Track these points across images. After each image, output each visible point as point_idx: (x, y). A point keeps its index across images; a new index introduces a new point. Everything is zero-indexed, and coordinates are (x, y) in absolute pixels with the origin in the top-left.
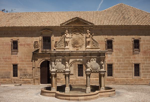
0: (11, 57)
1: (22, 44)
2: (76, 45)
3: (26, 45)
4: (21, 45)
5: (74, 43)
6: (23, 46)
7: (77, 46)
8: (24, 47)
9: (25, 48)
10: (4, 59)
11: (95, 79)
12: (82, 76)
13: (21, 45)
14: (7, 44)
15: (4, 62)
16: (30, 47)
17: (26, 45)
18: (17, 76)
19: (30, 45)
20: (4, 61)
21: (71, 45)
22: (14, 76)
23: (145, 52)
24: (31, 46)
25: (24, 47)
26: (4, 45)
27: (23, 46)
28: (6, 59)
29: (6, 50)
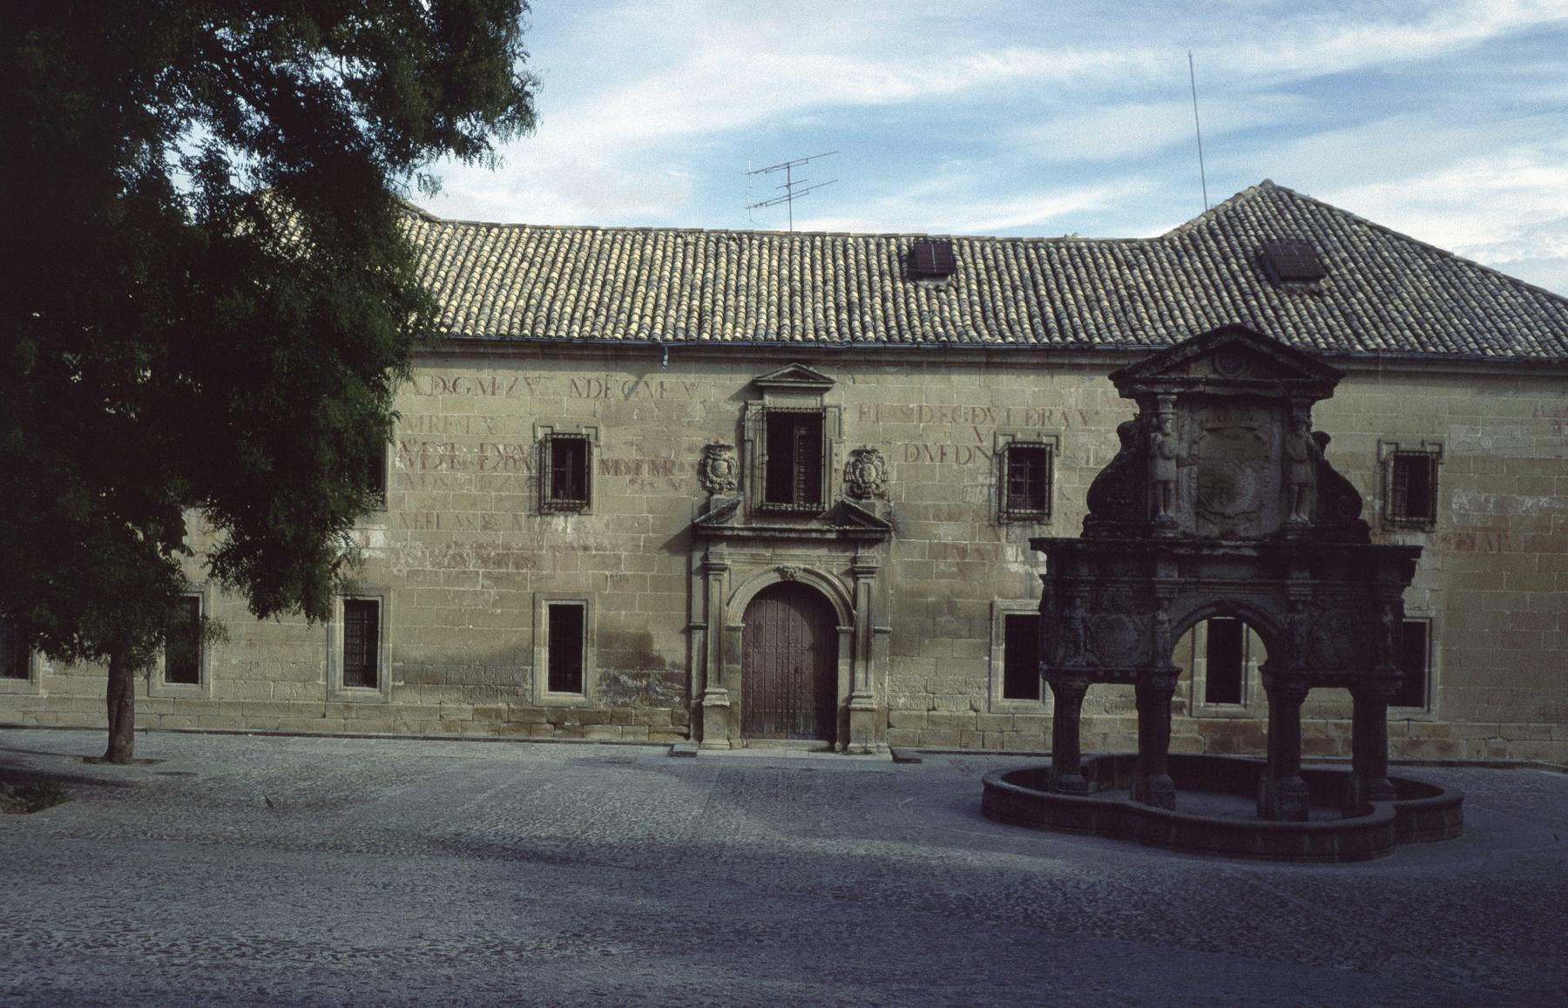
0: (541, 548)
1: (617, 462)
2: (1217, 507)
3: (645, 469)
4: (612, 467)
6: (628, 477)
7: (1229, 511)
8: (632, 481)
9: (636, 487)
10: (485, 561)
11: (1118, 717)
12: (1033, 694)
13: (612, 467)
14: (511, 462)
15: (487, 583)
16: (675, 487)
17: (645, 469)
18: (575, 685)
19: (675, 471)
20: (488, 576)
22: (555, 685)
23: (1464, 541)
24: (678, 476)
25: (632, 481)
26: (488, 465)
27: (628, 477)
28: (499, 564)
29: (500, 499)
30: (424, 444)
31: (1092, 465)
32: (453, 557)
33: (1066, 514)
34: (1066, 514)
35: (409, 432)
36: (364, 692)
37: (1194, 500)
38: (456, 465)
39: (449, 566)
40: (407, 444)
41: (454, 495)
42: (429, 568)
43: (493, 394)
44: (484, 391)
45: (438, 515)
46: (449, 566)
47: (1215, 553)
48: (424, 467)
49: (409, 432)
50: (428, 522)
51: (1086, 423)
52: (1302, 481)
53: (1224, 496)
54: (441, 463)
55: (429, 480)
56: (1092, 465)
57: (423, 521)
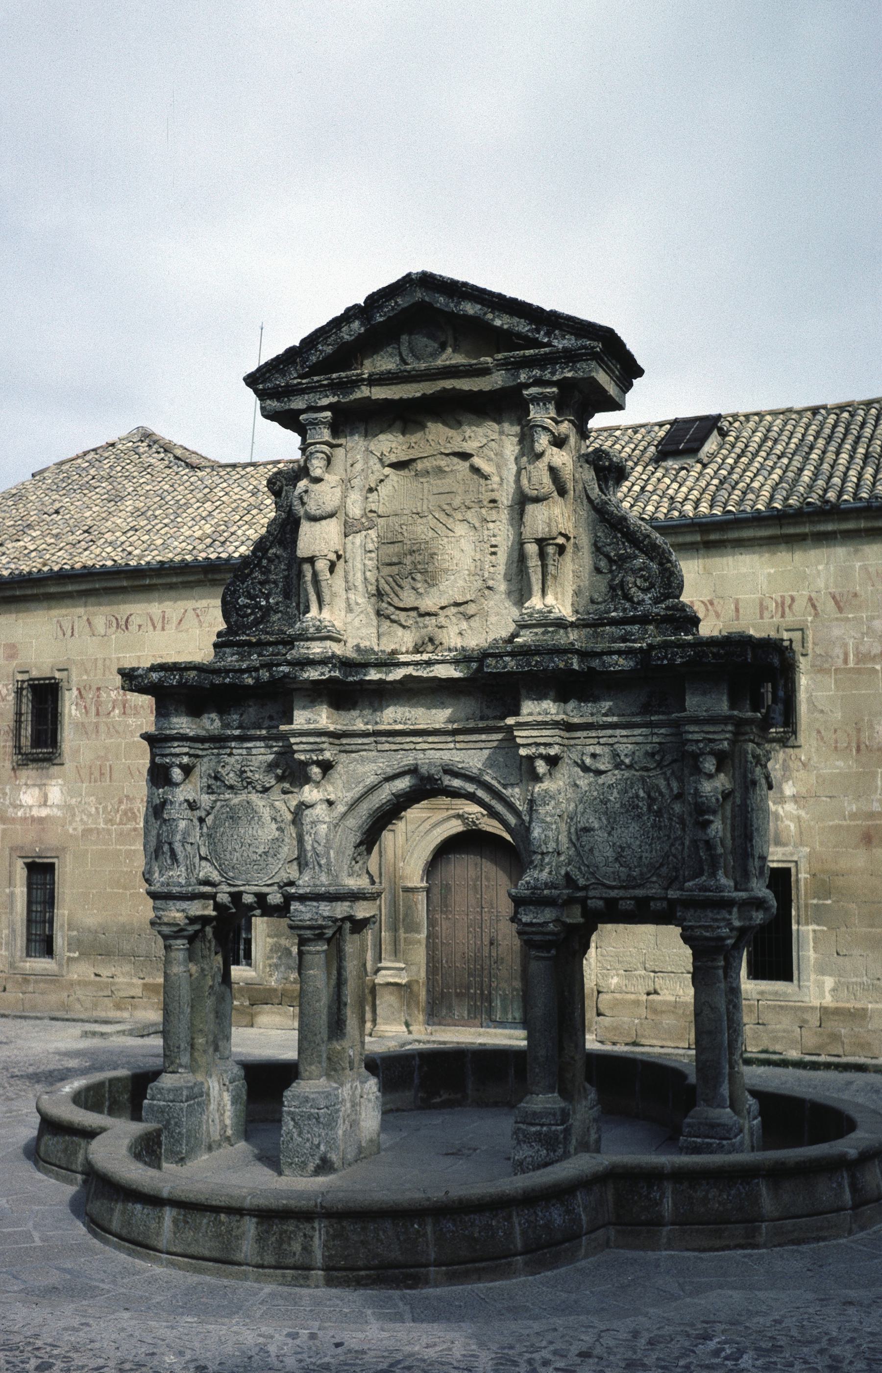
2: (408, 599)
5: (395, 569)
7: (428, 603)
21: (360, 598)
30: (99, 689)
31: (851, 665)
32: (125, 813)
33: (819, 732)
34: (819, 732)
35: (85, 677)
36: (42, 964)
37: (372, 589)
38: (128, 711)
39: (121, 823)
40: (83, 692)
41: (127, 743)
42: (102, 825)
43: (163, 629)
44: (155, 627)
45: (110, 766)
46: (121, 823)
47: (391, 677)
48: (98, 714)
49: (85, 677)
50: (102, 774)
51: (840, 609)
52: (540, 536)
53: (419, 577)
54: (114, 708)
55: (103, 728)
56: (851, 665)
57: (97, 774)
